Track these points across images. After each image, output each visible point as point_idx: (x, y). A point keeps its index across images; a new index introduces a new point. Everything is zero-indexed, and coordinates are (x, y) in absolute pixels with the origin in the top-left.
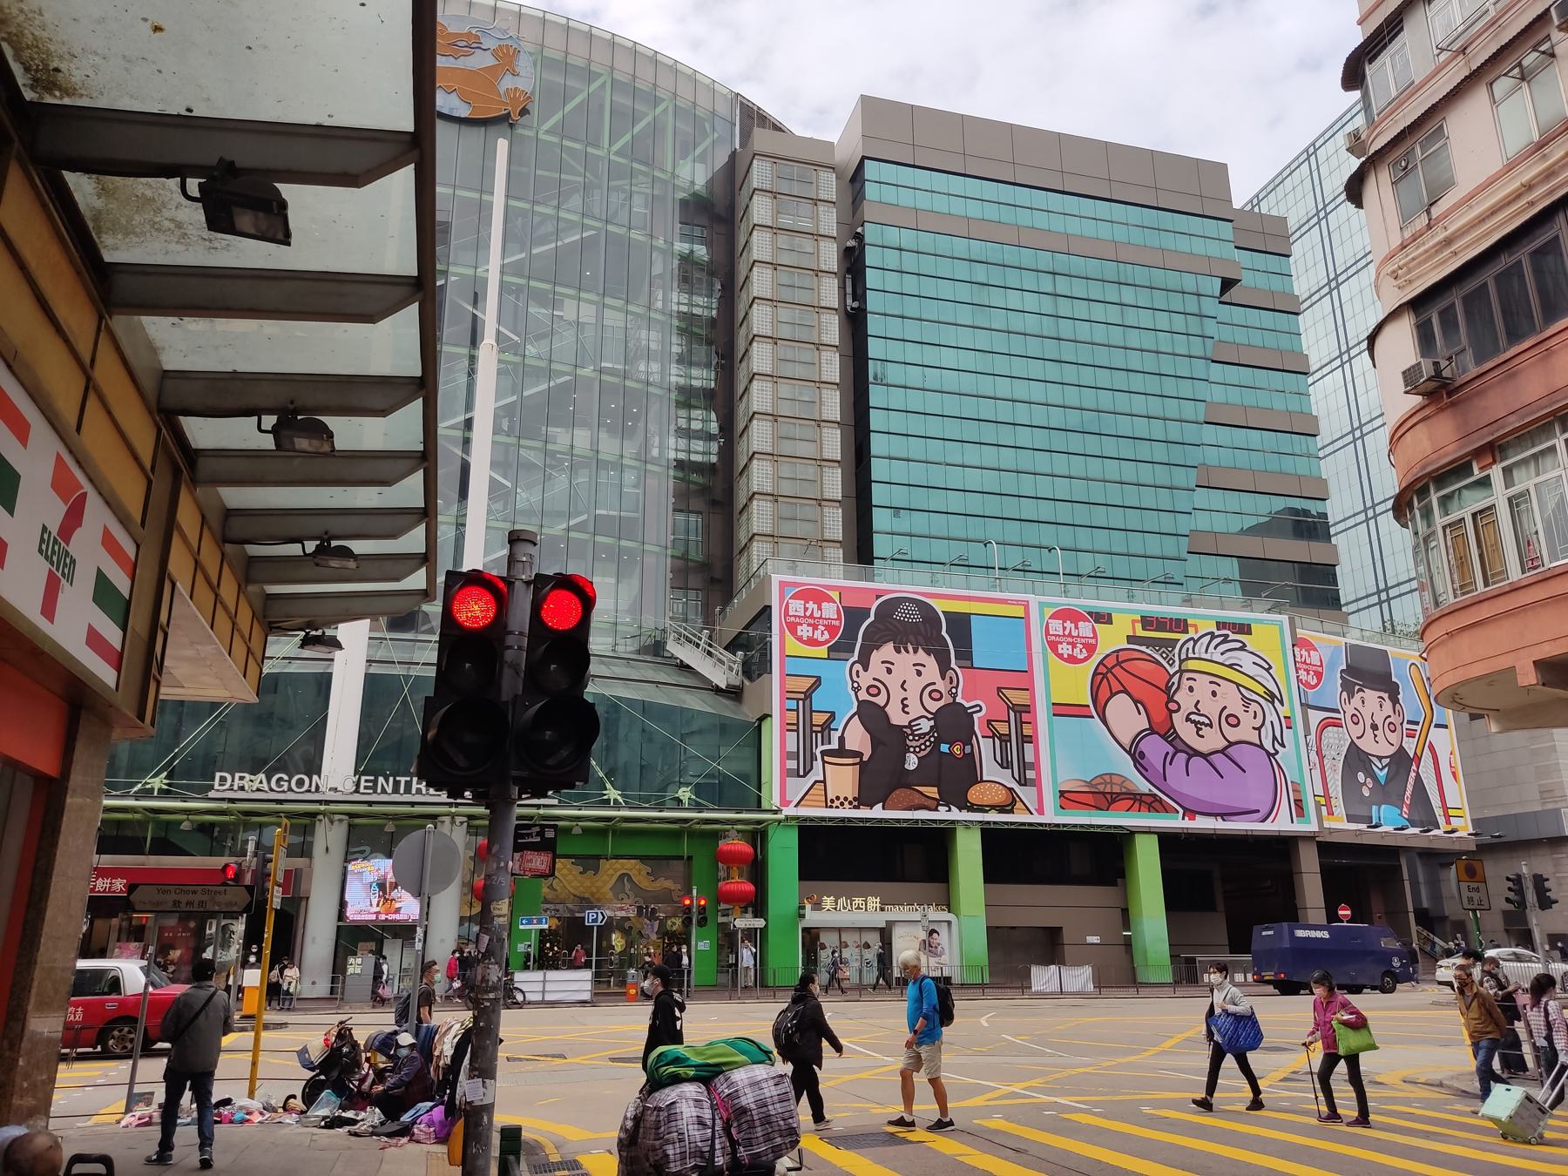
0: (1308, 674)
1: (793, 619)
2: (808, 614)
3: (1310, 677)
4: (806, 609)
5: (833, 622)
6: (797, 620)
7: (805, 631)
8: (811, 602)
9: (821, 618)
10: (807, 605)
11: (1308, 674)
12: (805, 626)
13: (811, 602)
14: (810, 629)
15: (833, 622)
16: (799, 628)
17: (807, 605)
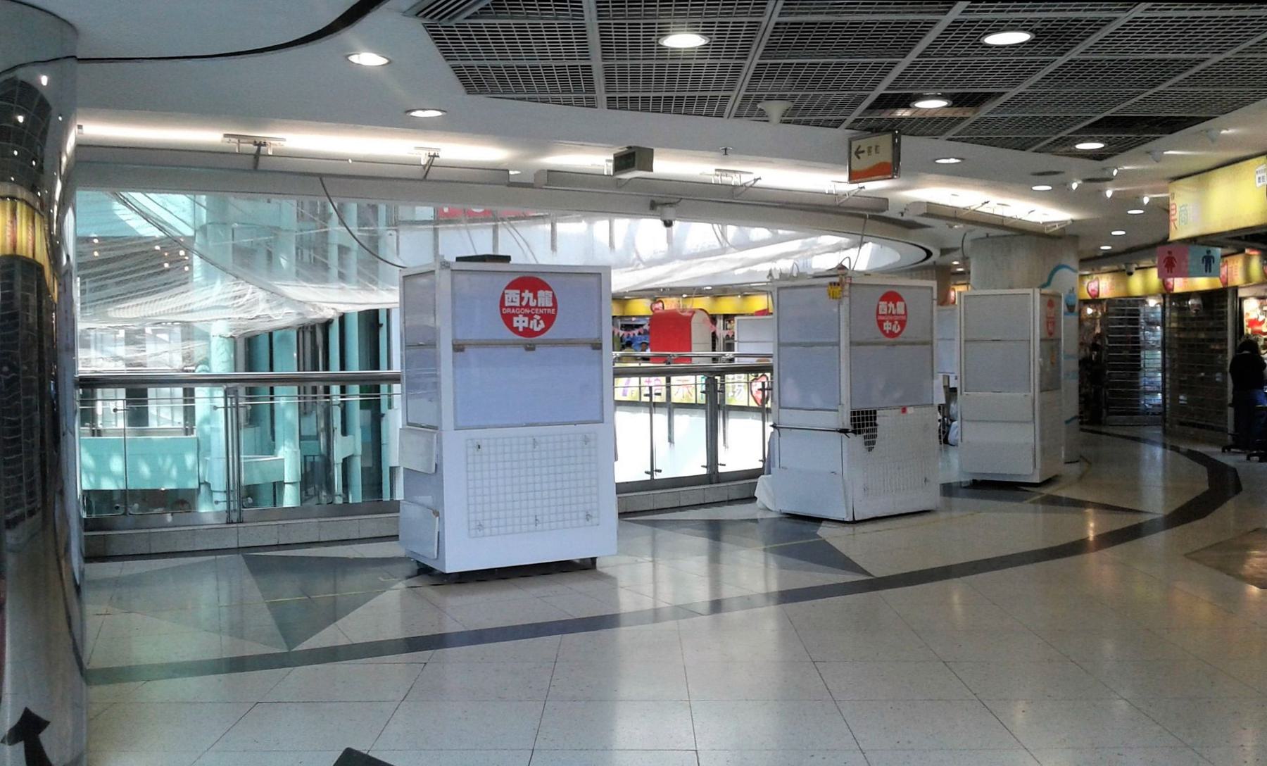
0: (893, 324)
1: (508, 311)
2: (524, 303)
3: (895, 327)
4: (522, 299)
5: (549, 310)
6: (513, 311)
7: (521, 322)
8: (527, 291)
9: (536, 307)
10: (523, 295)
11: (893, 324)
12: (520, 316)
13: (527, 291)
14: (526, 319)
15: (549, 310)
16: (515, 319)
17: (523, 295)
